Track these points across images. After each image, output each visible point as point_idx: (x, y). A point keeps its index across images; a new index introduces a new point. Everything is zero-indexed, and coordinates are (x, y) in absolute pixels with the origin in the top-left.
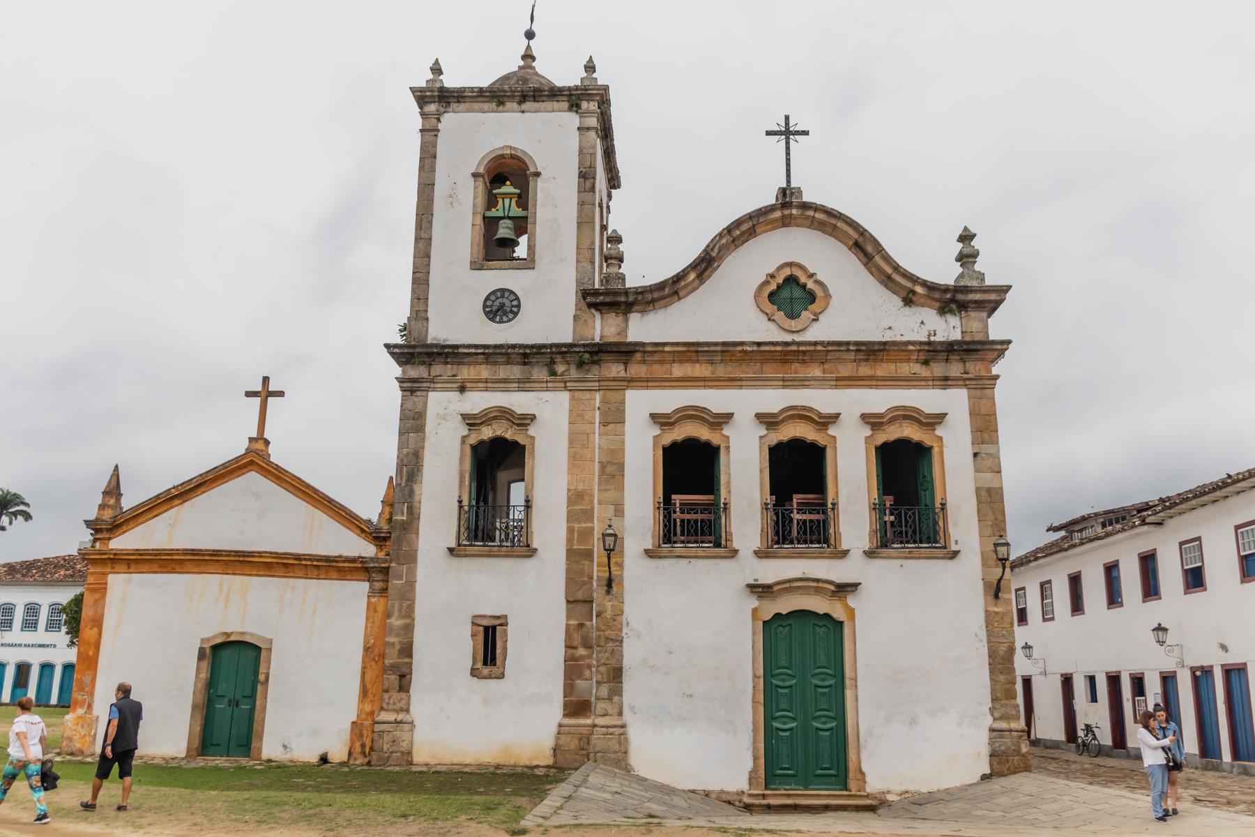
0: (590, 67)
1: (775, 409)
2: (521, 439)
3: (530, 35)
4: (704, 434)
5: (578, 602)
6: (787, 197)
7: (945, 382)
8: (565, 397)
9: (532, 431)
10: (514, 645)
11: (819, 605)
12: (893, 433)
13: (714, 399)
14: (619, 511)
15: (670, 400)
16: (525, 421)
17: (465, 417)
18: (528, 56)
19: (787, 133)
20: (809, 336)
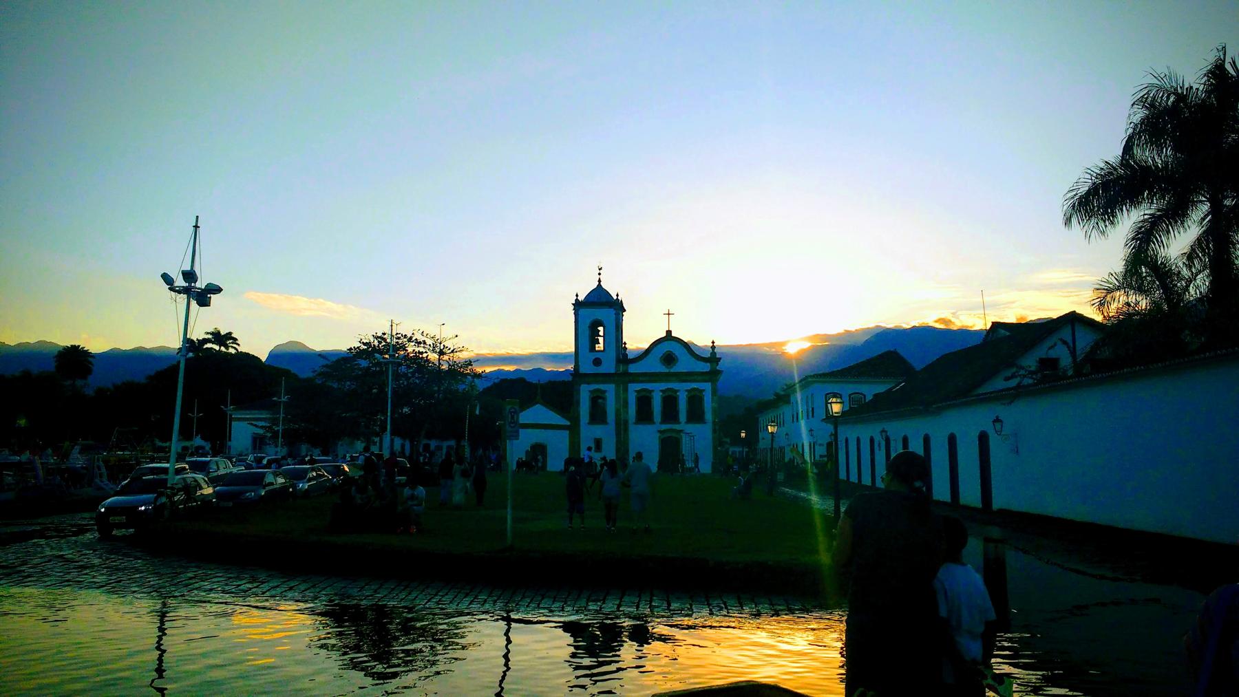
0: (617, 295)
1: (664, 388)
2: (603, 396)
3: (599, 274)
4: (648, 394)
5: (618, 434)
6: (669, 332)
7: (706, 381)
8: (614, 385)
9: (607, 394)
10: (604, 446)
11: (674, 435)
12: (693, 393)
13: (648, 386)
14: (627, 413)
15: (639, 386)
16: (604, 392)
17: (590, 391)
18: (600, 281)
19: (669, 314)
20: (672, 371)
